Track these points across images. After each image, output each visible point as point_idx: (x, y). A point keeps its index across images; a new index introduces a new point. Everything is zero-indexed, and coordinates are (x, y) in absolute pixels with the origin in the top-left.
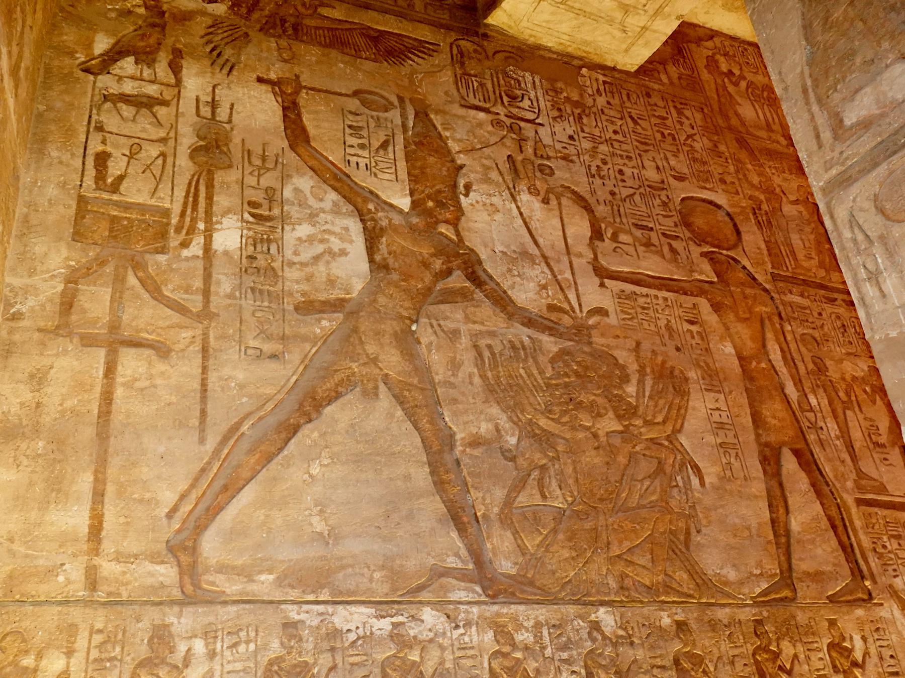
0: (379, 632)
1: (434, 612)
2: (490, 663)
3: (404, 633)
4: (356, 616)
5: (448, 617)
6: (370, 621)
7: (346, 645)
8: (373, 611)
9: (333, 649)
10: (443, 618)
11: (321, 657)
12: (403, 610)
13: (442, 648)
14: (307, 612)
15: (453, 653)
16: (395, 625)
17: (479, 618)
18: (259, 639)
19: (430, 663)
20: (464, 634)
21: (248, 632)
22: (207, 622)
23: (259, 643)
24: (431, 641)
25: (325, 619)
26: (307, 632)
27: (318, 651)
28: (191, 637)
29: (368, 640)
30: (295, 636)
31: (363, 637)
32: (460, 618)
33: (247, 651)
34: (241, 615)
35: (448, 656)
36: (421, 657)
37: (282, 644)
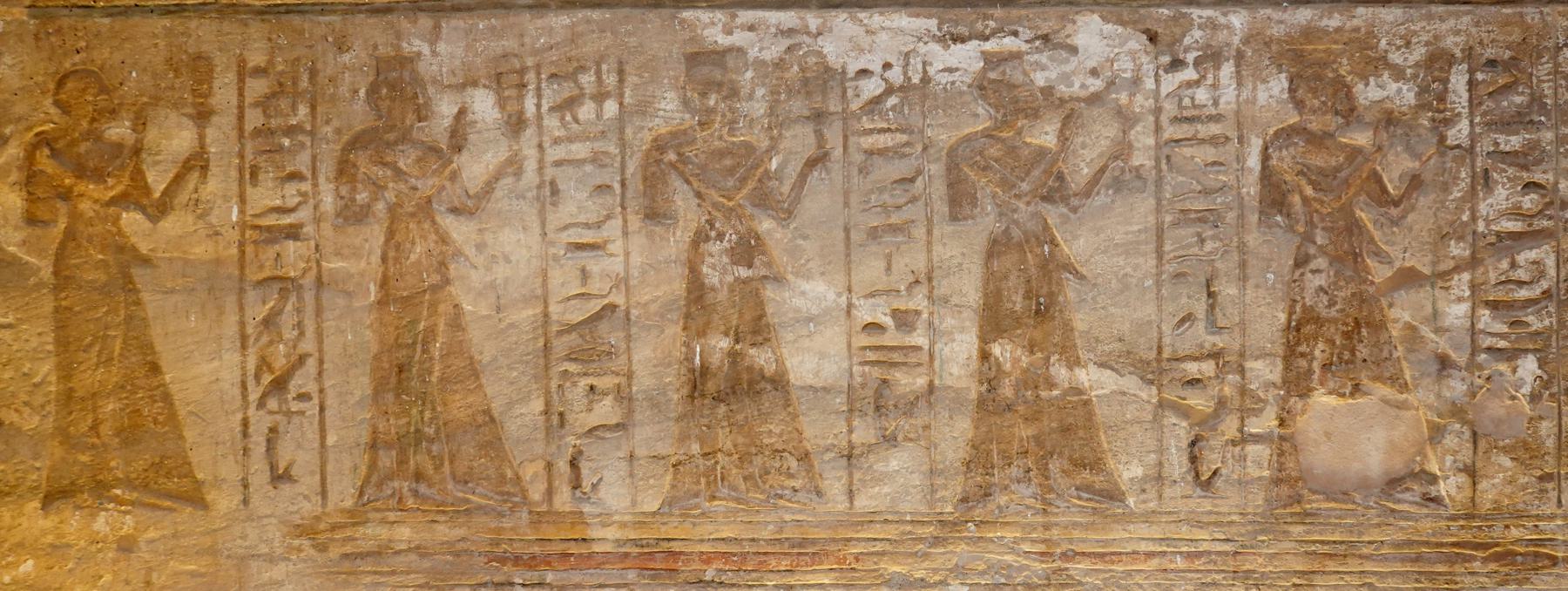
0: (945, 78)
1: (1109, 28)
2: (1265, 157)
3: (1018, 77)
4: (883, 37)
5: (1153, 38)
6: (922, 48)
7: (854, 106)
8: (932, 24)
9: (818, 117)
10: (1137, 42)
11: (787, 134)
12: (1019, 21)
13: (1126, 119)
14: (751, 28)
15: (1158, 129)
16: (991, 60)
17: (1246, 41)
18: (628, 92)
19: (1088, 154)
20: (1197, 83)
21: (598, 73)
22: (499, 51)
23: (627, 100)
24: (1094, 99)
25: (799, 45)
26: (749, 74)
27: (777, 122)
28: (464, 86)
29: (915, 97)
30: (720, 85)
31: (901, 88)
32: (1187, 41)
33: (599, 116)
34: (582, 35)
35: (1143, 138)
36: (1063, 138)
37: (686, 103)
